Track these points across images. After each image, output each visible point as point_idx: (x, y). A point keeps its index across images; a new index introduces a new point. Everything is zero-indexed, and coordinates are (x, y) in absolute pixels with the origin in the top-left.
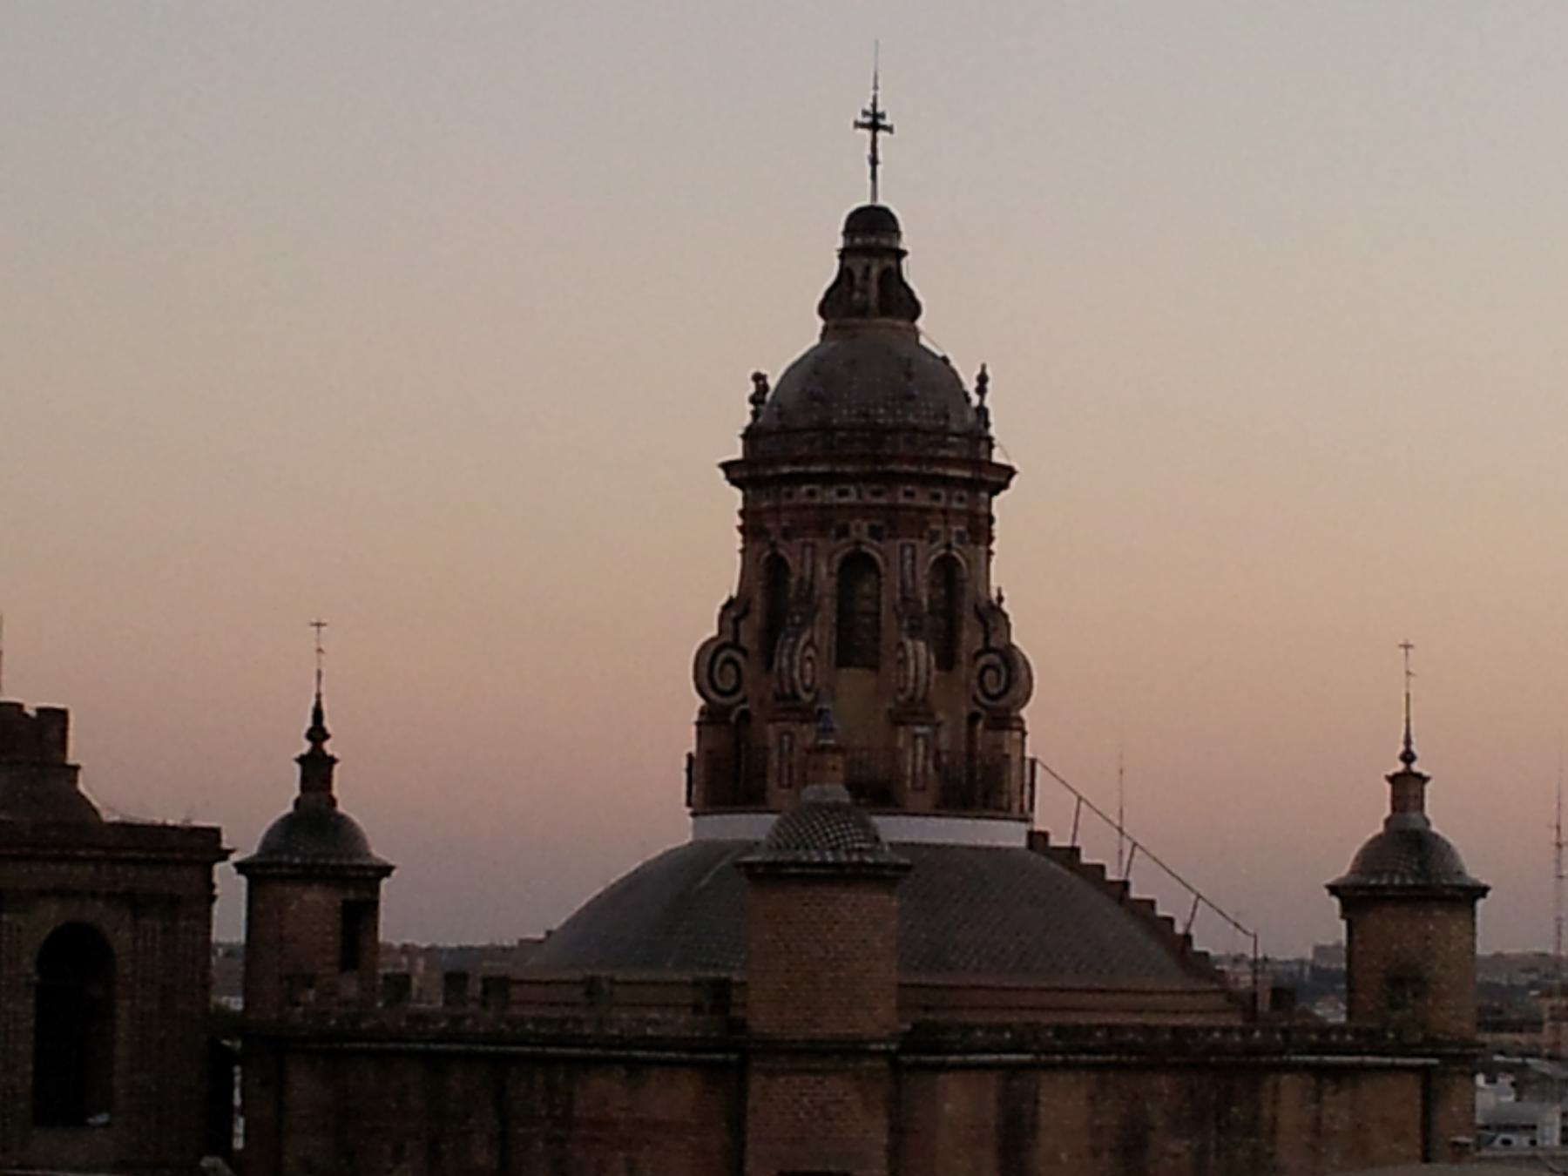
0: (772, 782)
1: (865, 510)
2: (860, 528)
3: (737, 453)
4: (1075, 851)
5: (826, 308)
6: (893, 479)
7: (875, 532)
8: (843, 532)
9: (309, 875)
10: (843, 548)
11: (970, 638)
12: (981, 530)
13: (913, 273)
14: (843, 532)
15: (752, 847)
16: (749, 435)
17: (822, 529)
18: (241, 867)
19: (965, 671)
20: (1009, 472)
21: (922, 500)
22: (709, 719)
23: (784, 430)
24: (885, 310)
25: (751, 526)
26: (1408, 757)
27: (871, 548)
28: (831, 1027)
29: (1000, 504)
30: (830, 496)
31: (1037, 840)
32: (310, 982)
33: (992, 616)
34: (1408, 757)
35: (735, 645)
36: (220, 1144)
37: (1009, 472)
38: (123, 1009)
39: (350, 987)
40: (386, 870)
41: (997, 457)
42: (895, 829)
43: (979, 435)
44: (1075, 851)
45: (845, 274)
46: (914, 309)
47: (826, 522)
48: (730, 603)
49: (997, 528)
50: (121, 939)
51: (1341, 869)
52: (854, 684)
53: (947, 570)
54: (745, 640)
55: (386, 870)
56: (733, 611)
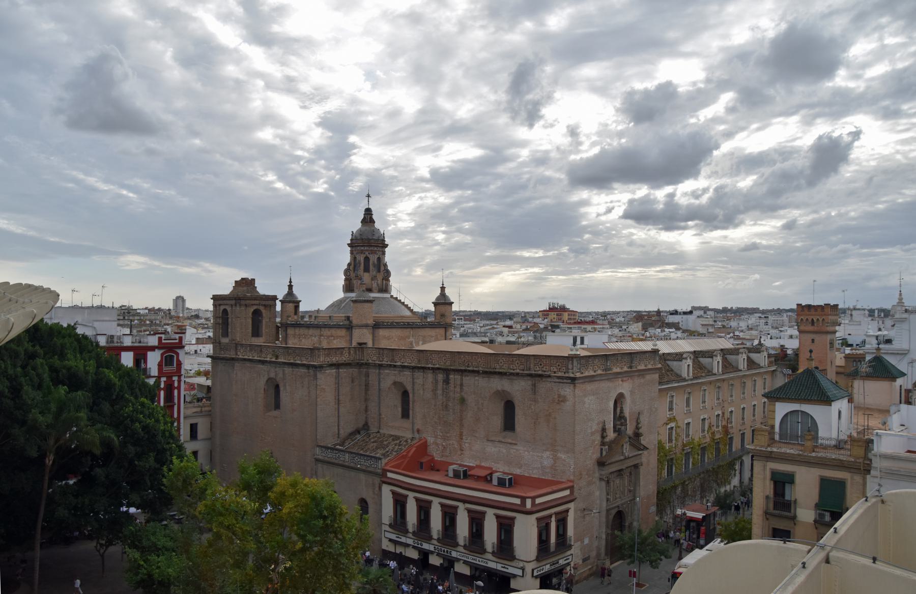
0: (355, 289)
1: (367, 250)
2: (367, 253)
3: (349, 242)
4: (397, 298)
5: (362, 222)
6: (371, 246)
7: (369, 253)
8: (364, 253)
9: (290, 302)
10: (365, 256)
11: (382, 268)
12: (384, 253)
13: (374, 217)
14: (364, 253)
15: (353, 297)
16: (351, 240)
17: (362, 253)
18: (280, 301)
19: (382, 273)
20: (388, 245)
21: (376, 249)
22: (346, 280)
23: (356, 239)
24: (370, 222)
25: (352, 253)
26: (443, 284)
27: (368, 256)
28: (364, 322)
29: (386, 250)
30: (362, 248)
31: (392, 296)
32: (290, 316)
33: (385, 265)
34: (443, 284)
35: (349, 269)
36: (278, 340)
37: (388, 245)
38: (264, 321)
39: (296, 317)
40: (300, 301)
41: (386, 243)
42: (373, 295)
43: (384, 240)
44: (397, 298)
45: (364, 217)
46: (374, 222)
47: (362, 252)
48: (349, 264)
49: (386, 253)
50: (263, 311)
51: (434, 300)
52: (366, 274)
53: (379, 259)
54: (351, 269)
55: (300, 301)
56: (349, 265)
